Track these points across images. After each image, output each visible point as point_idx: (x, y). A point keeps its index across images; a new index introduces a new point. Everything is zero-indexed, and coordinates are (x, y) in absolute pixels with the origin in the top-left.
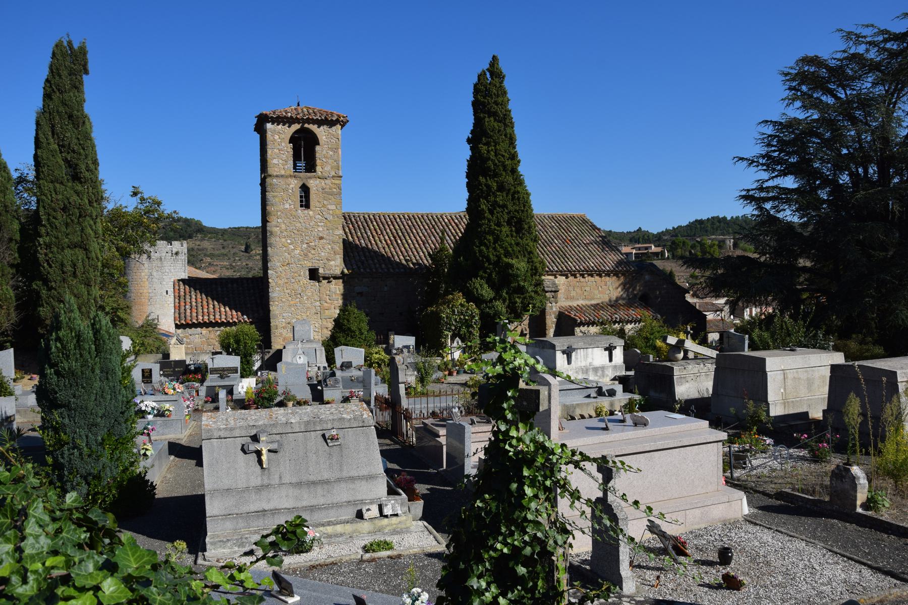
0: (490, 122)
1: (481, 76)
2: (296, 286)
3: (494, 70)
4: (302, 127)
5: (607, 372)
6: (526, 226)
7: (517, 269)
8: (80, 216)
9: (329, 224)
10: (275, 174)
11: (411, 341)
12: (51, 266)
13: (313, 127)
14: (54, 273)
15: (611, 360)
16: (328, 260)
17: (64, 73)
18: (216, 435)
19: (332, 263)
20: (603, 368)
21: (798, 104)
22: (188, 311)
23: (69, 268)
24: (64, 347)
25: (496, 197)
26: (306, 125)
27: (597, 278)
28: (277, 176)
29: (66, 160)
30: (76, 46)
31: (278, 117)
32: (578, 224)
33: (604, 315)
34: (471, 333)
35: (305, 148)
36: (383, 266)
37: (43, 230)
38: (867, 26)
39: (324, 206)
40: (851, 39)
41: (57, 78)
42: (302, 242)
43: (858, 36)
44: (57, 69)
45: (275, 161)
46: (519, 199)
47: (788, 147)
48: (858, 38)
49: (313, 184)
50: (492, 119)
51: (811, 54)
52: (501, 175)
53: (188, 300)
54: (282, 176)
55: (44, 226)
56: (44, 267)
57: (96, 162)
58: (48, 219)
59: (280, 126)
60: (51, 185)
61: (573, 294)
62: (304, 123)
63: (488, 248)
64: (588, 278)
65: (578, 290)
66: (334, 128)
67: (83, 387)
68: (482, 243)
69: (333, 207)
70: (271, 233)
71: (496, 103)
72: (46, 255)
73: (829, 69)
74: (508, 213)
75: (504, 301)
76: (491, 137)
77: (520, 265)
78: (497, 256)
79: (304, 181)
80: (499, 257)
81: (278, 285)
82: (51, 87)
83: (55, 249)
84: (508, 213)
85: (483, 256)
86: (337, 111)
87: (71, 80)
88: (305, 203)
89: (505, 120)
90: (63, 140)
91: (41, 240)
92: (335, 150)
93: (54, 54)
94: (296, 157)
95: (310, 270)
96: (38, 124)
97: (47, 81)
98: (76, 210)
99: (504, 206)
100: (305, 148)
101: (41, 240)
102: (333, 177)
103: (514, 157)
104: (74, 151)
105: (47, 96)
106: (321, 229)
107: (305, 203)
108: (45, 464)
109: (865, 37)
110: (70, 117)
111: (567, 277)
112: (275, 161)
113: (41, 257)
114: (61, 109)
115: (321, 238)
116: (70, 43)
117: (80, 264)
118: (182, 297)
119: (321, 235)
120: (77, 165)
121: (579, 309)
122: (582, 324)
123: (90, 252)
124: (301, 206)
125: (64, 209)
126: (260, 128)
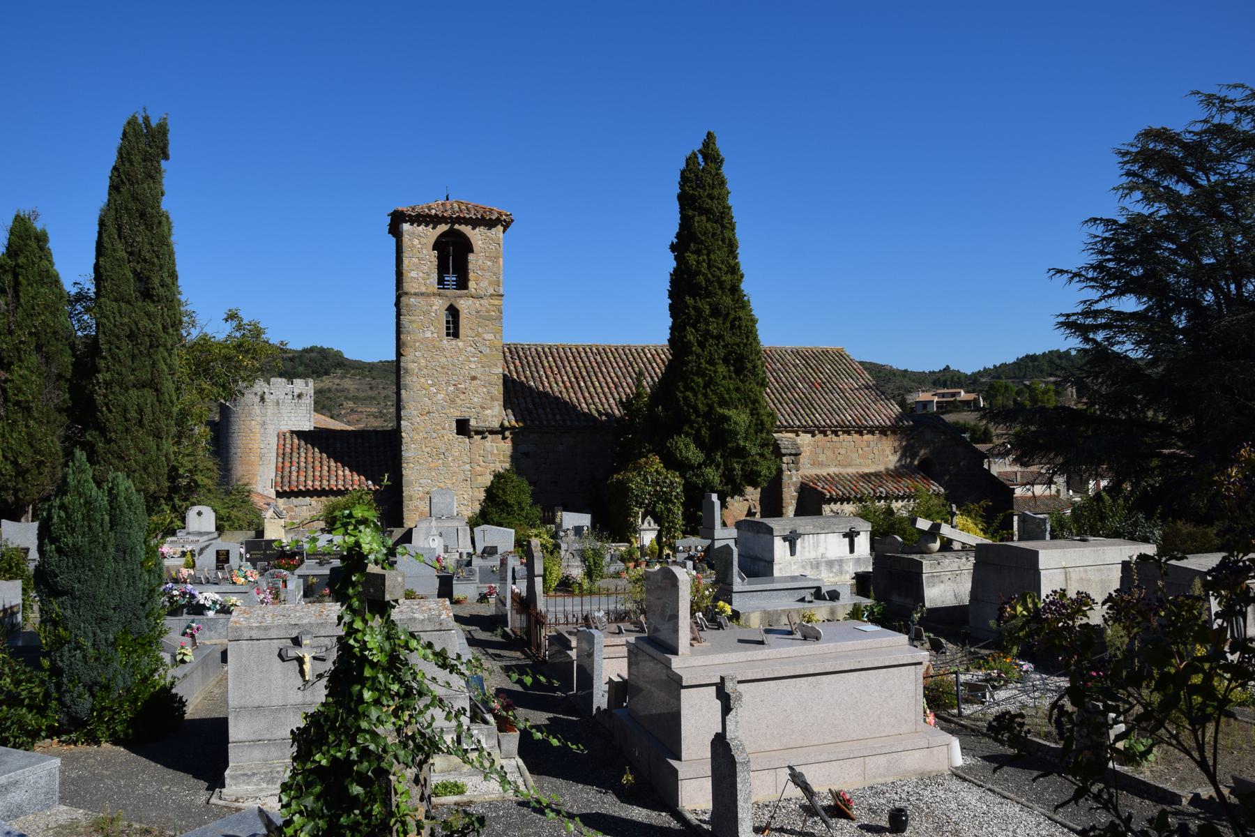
0: (700, 222)
1: (691, 160)
2: (438, 443)
3: (709, 153)
4: (451, 228)
5: (846, 567)
6: (749, 366)
7: (736, 423)
8: (151, 346)
9: (484, 360)
11: (584, 520)
12: (110, 412)
13: (466, 229)
14: (113, 420)
15: (852, 550)
16: (482, 408)
17: (137, 159)
18: (246, 635)
19: (488, 412)
20: (841, 562)
21: (1138, 195)
22: (294, 474)
23: (133, 414)
24: (69, 517)
25: (708, 324)
26: (456, 226)
27: (856, 436)
28: (415, 294)
29: (134, 271)
30: (154, 123)
31: (419, 215)
32: (833, 362)
33: (866, 489)
34: (669, 510)
35: (453, 257)
36: (558, 417)
37: (102, 364)
38: (1235, 87)
39: (478, 335)
40: (1214, 105)
41: (127, 165)
42: (448, 383)
43: (1223, 101)
44: (128, 153)
45: (413, 274)
46: (740, 327)
47: (1127, 255)
48: (1224, 104)
49: (464, 305)
50: (704, 218)
51: (1157, 126)
52: (716, 294)
53: (295, 459)
54: (422, 294)
55: (105, 358)
56: (101, 412)
57: (173, 275)
58: (110, 349)
59: (420, 228)
60: (115, 305)
61: (822, 458)
63: (695, 395)
64: (843, 437)
65: (829, 453)
66: (494, 230)
67: (91, 570)
68: (688, 388)
69: (490, 336)
70: (407, 371)
71: (711, 197)
72: (105, 396)
73: (1184, 146)
74: (725, 347)
75: (718, 466)
76: (702, 242)
77: (740, 418)
78: (708, 405)
79: (452, 301)
80: (711, 407)
81: (413, 441)
82: (119, 176)
83: (117, 389)
84: (725, 347)
85: (689, 406)
86: (498, 207)
87: (145, 167)
88: (453, 329)
89: (723, 219)
90: (132, 246)
91: (100, 376)
92: (495, 259)
93: (125, 134)
94: (442, 269)
95: (458, 421)
96: (102, 224)
97: (115, 168)
98: (147, 339)
99: (719, 337)
100: (453, 257)
101: (100, 376)
102: (491, 295)
103: (734, 270)
104: (145, 261)
105: (114, 188)
106: (473, 366)
107: (453, 329)
108: (40, 667)
109: (1233, 101)
110: (142, 215)
111: (814, 436)
112: (413, 274)
113: (99, 399)
114: (132, 205)
115: (474, 378)
116: (146, 119)
117: (148, 410)
118: (288, 455)
119: (473, 374)
120: (148, 278)
121: (831, 480)
122: (832, 500)
123: (163, 394)
124: (448, 335)
125: (131, 336)
126: (395, 230)
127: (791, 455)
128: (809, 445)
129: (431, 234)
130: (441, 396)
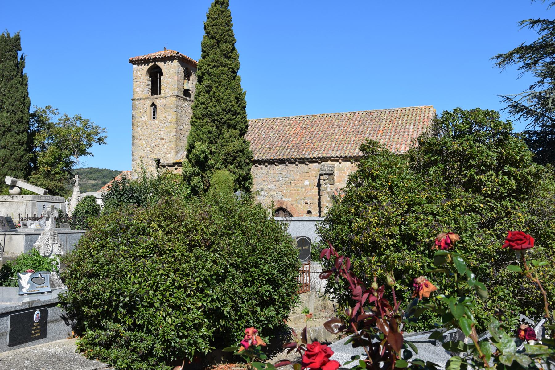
10: (137, 98)
13: (159, 64)
19: (168, 156)
28: (138, 99)
30: (12, 36)
45: (137, 90)
49: (158, 102)
62: (155, 62)
102: (171, 96)
111: (352, 163)
112: (137, 90)
115: (163, 139)
116: (8, 34)
119: (163, 137)
127: (326, 174)
128: (348, 169)
129: (145, 68)
130: (148, 149)
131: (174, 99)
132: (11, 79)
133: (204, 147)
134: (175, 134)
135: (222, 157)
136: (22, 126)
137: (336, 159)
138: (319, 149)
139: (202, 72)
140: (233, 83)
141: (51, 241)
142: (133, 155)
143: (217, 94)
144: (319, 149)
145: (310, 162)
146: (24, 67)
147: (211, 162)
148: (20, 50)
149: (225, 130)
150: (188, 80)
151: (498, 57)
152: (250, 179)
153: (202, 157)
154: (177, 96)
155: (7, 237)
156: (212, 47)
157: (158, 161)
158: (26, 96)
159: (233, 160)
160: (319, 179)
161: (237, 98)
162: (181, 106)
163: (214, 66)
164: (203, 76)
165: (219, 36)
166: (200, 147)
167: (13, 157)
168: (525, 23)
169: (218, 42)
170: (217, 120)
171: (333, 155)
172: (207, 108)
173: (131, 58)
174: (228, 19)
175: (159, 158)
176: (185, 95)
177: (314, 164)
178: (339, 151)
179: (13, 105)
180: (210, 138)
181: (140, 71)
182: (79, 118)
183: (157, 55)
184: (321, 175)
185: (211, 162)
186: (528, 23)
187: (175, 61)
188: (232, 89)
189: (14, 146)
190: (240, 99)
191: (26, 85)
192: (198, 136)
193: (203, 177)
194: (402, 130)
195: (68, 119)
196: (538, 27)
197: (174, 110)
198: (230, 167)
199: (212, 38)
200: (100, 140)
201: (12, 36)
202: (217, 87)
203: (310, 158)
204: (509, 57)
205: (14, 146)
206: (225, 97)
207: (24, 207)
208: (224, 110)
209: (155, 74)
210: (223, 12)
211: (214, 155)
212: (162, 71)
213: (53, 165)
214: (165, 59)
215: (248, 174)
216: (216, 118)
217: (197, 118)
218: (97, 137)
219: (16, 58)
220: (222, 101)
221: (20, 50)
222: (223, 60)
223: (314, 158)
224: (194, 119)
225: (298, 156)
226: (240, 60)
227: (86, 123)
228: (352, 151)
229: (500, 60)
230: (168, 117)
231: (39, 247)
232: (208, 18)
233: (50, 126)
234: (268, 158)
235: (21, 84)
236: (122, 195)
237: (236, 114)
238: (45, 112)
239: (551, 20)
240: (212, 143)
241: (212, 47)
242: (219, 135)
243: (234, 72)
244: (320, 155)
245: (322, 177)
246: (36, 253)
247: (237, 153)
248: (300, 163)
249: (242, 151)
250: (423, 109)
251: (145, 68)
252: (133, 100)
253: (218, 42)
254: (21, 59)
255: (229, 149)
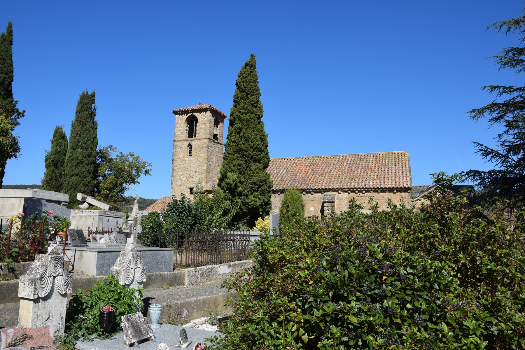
3: (250, 65)
13: (195, 114)
30: (90, 93)
45: (178, 133)
49: (194, 143)
59: (181, 116)
62: (193, 113)
79: (190, 142)
111: (349, 194)
112: (178, 133)
115: (196, 172)
116: (87, 92)
127: (328, 202)
128: (346, 198)
129: (185, 117)
130: (184, 179)
131: (206, 141)
132: (86, 124)
133: (235, 177)
134: (206, 168)
135: (249, 186)
136: (91, 160)
137: (336, 190)
138: (321, 182)
139: (234, 118)
140: (258, 127)
141: (132, 265)
142: (172, 184)
143: (246, 135)
144: (321, 182)
145: (315, 192)
146: (95, 116)
147: (240, 189)
148: (94, 103)
149: (252, 164)
150: (217, 127)
151: (472, 112)
152: (270, 204)
153: (233, 185)
154: (209, 139)
155: (78, 253)
156: (242, 98)
157: (191, 189)
158: (95, 137)
159: (258, 188)
160: (323, 206)
161: (262, 139)
162: (211, 146)
163: (244, 113)
164: (234, 120)
165: (247, 92)
166: (232, 177)
167: (83, 182)
168: (487, 89)
169: (248, 94)
170: (246, 155)
171: (334, 187)
172: (237, 146)
173: (174, 110)
174: (256, 77)
175: (192, 186)
176: (214, 138)
177: (318, 194)
178: (339, 184)
179: (85, 144)
180: (239, 169)
181: (180, 119)
182: (132, 155)
183: (194, 107)
184: (325, 202)
185: (240, 189)
186: (489, 88)
187: (208, 112)
188: (258, 131)
189: (84, 174)
190: (263, 139)
191: (96, 129)
192: (230, 168)
193: (232, 201)
194: (387, 169)
195: (123, 156)
196: (496, 91)
197: (206, 149)
198: (256, 194)
199: (243, 91)
200: (146, 172)
201: (90, 93)
202: (246, 129)
203: (315, 189)
204: (480, 112)
205: (84, 174)
206: (253, 137)
207: (92, 220)
208: (251, 147)
209: (192, 122)
210: (251, 72)
211: (242, 184)
212: (197, 120)
213: (111, 190)
214: (200, 111)
215: (269, 200)
216: (245, 153)
217: (229, 154)
218: (144, 170)
219: (91, 109)
220: (250, 140)
221: (94, 103)
222: (250, 108)
223: (319, 189)
224: (227, 155)
225: (305, 187)
226: (264, 109)
227: (137, 159)
228: (349, 184)
229: (473, 114)
230: (201, 155)
231: (118, 273)
232: (239, 77)
233: (111, 160)
234: (281, 188)
235: (93, 129)
236: (182, 213)
237: (261, 151)
238: (108, 150)
239: (507, 86)
240: (241, 174)
241: (242, 98)
242: (247, 167)
243: (259, 118)
244: (323, 187)
245: (325, 205)
246: (113, 282)
247: (261, 182)
248: (307, 193)
249: (265, 181)
250: (400, 154)
251: (185, 117)
252: (174, 141)
253: (248, 94)
254: (94, 110)
255: (255, 179)
